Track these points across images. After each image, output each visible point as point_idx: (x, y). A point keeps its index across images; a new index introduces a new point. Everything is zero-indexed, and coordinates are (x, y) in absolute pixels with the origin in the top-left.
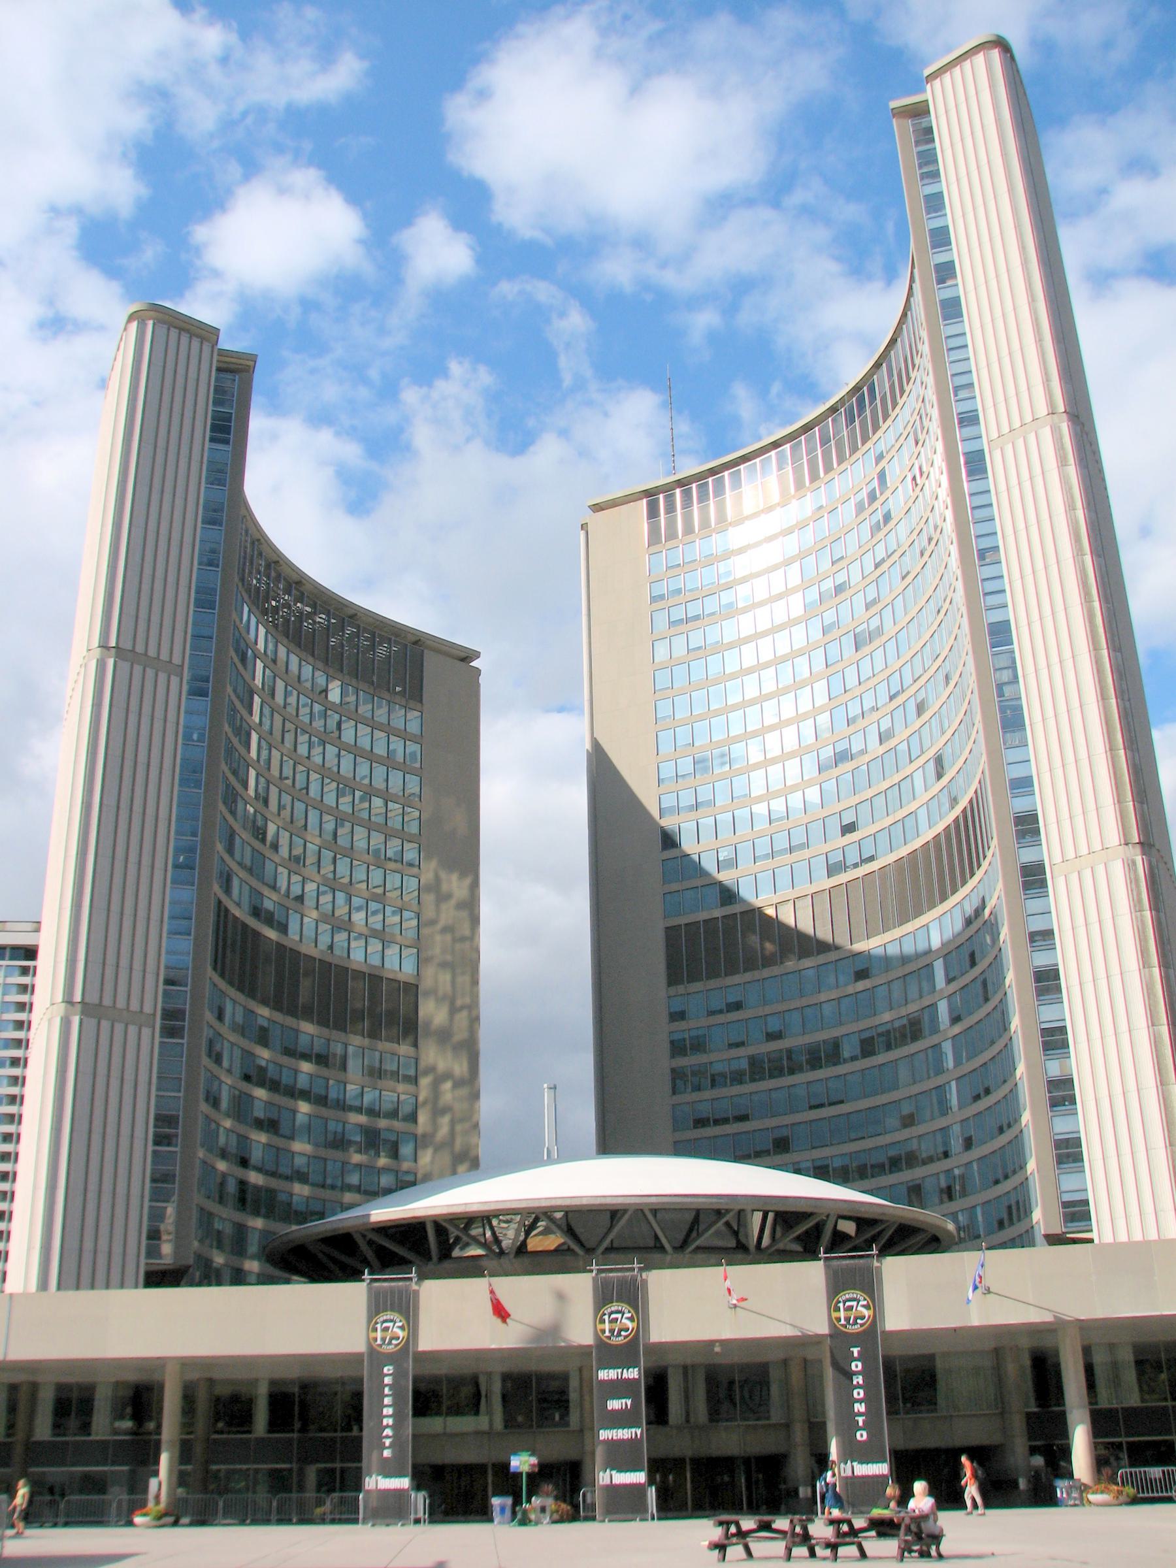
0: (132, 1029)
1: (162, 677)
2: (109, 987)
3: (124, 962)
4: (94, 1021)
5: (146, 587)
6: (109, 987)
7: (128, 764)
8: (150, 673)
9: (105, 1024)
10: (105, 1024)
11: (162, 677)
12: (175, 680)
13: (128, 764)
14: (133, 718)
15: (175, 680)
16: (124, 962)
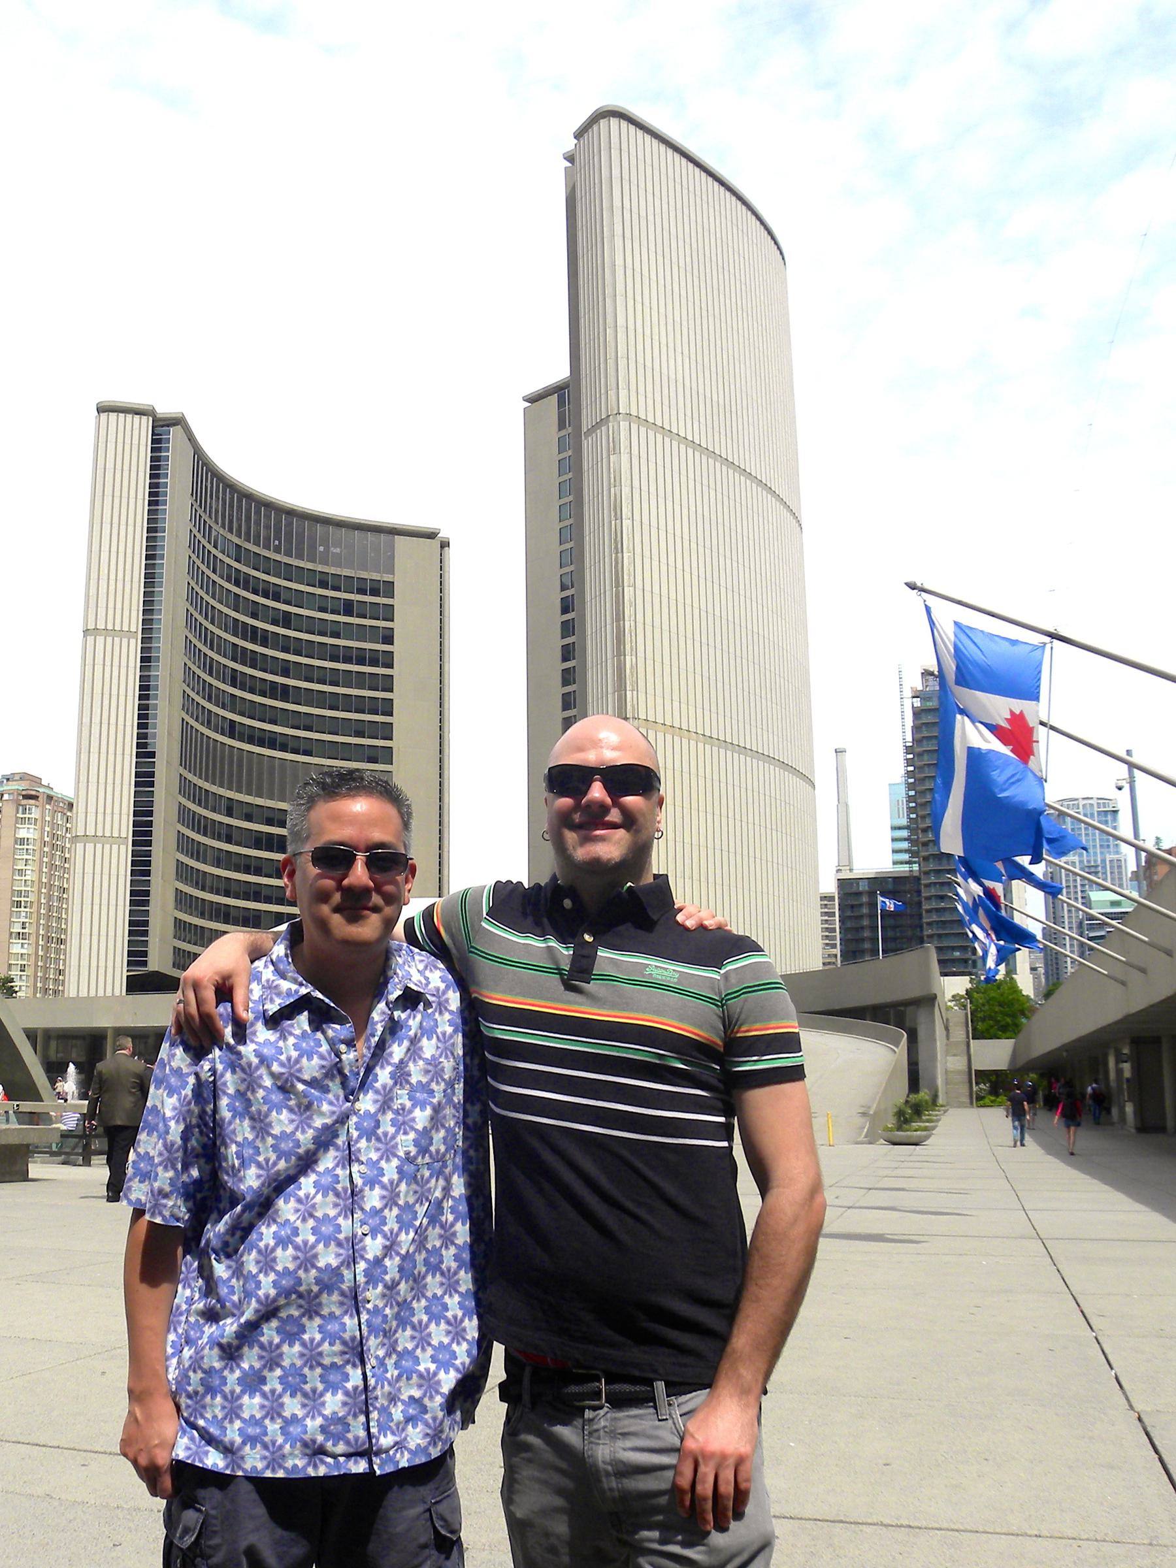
0: (115, 847)
1: (125, 641)
2: (100, 826)
3: (109, 811)
4: (92, 845)
5: (112, 588)
6: (100, 826)
7: (106, 697)
8: (117, 640)
9: (99, 846)
10: (99, 846)
11: (125, 641)
12: (133, 641)
13: (106, 697)
14: (108, 669)
15: (133, 641)
16: (109, 811)
